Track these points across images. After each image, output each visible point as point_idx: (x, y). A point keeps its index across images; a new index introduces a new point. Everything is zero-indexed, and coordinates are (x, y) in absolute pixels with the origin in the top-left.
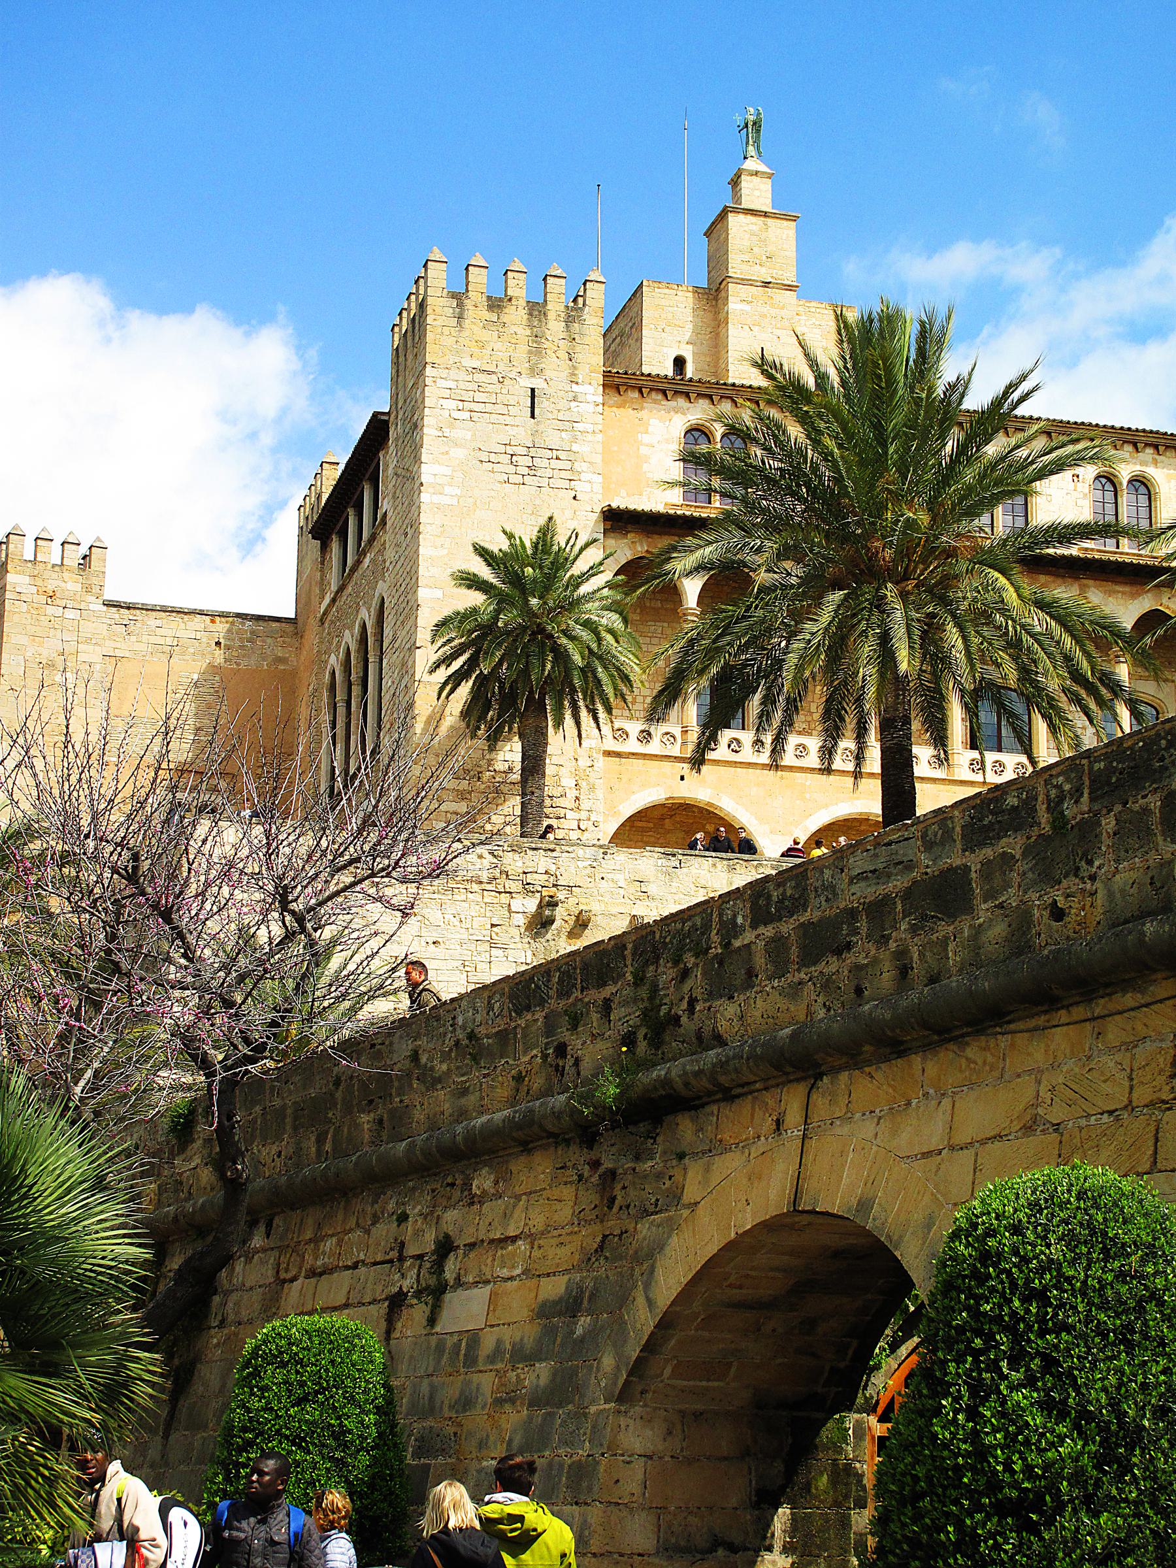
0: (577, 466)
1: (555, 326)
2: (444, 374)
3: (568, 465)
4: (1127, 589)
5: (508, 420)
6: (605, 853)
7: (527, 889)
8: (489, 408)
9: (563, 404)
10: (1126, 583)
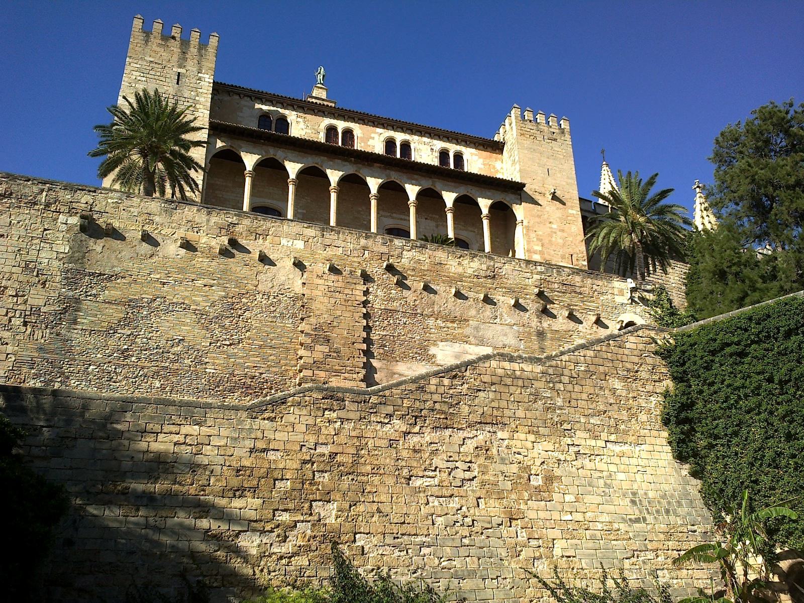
0: (198, 106)
1: (193, 50)
4: (453, 184)
5: (165, 84)
9: (194, 80)
10: (452, 182)
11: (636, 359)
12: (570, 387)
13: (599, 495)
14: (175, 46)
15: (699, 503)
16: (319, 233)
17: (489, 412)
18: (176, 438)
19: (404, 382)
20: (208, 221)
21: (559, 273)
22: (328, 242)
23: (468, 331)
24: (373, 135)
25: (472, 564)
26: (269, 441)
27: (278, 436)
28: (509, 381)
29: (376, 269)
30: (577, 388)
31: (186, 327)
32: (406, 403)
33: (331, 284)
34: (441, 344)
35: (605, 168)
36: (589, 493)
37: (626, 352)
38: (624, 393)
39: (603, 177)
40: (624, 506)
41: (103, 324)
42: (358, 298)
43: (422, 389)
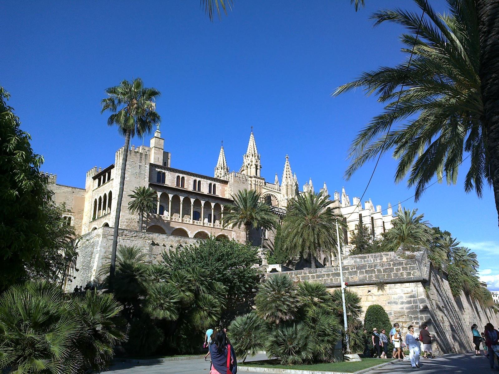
0: (145, 177)
1: (143, 157)
7: (149, 239)
35: (252, 135)
39: (250, 140)
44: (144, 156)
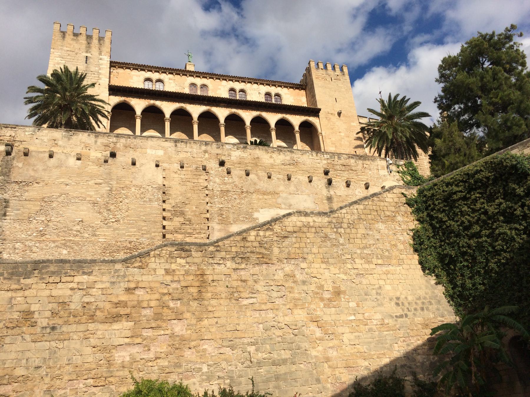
0: (100, 76)
1: (95, 41)
2: (57, 51)
3: (97, 76)
6: (39, 130)
8: (71, 60)
11: (393, 209)
12: (348, 230)
13: (373, 301)
14: (82, 39)
15: (444, 301)
16: (173, 144)
17: (293, 251)
18: (71, 285)
19: (232, 235)
20: (96, 142)
21: (339, 158)
22: (179, 149)
23: (279, 200)
24: (220, 87)
25: (286, 355)
26: (138, 282)
27: (145, 278)
28: (305, 230)
29: (213, 165)
30: (354, 231)
31: (85, 212)
32: (234, 249)
33: (183, 177)
34: (261, 210)
36: (366, 300)
37: (386, 204)
38: (386, 231)
40: (390, 308)
41: (24, 215)
42: (202, 184)
43: (244, 239)
44: (97, 41)
